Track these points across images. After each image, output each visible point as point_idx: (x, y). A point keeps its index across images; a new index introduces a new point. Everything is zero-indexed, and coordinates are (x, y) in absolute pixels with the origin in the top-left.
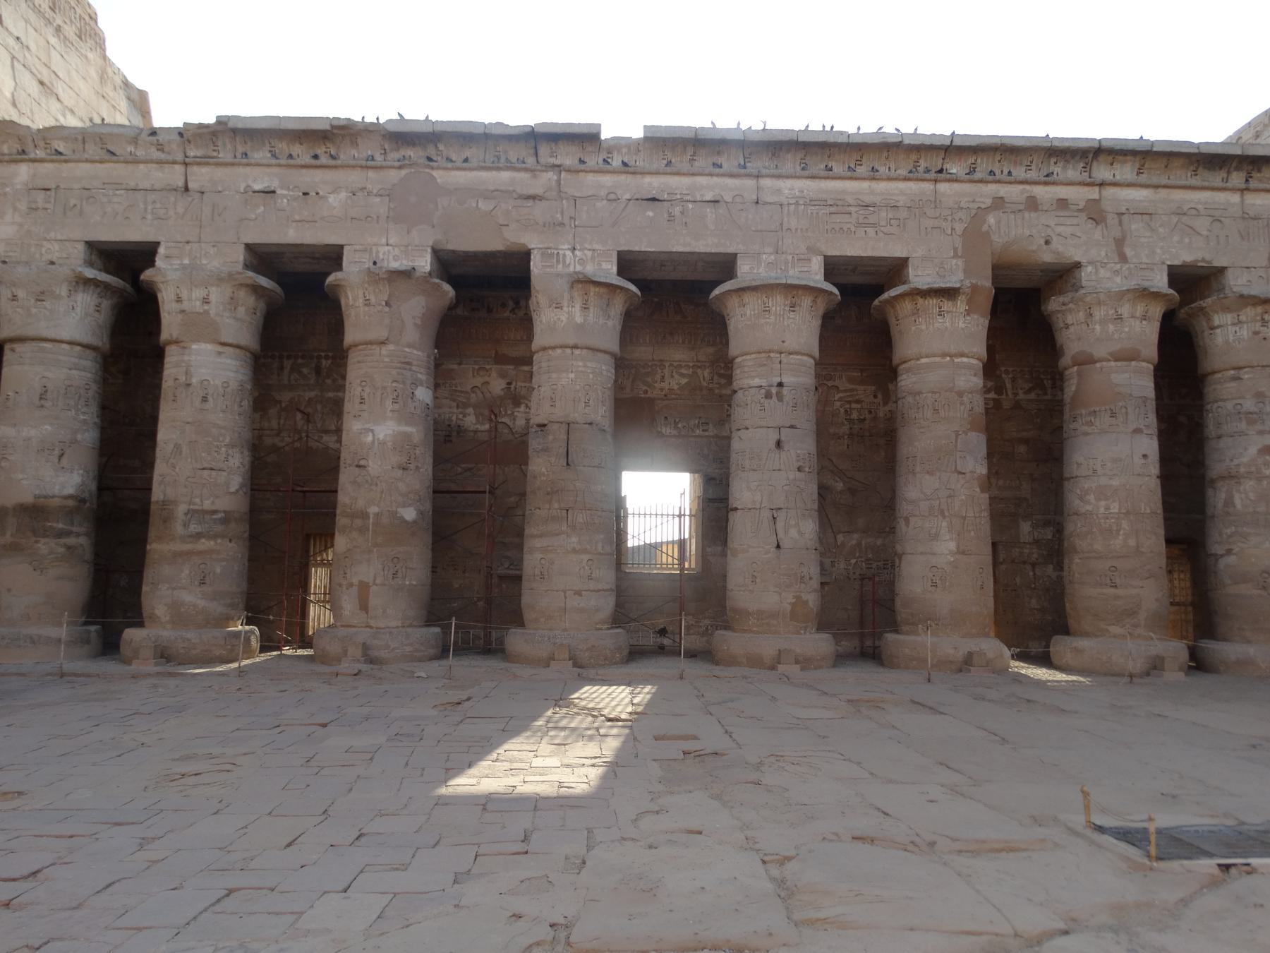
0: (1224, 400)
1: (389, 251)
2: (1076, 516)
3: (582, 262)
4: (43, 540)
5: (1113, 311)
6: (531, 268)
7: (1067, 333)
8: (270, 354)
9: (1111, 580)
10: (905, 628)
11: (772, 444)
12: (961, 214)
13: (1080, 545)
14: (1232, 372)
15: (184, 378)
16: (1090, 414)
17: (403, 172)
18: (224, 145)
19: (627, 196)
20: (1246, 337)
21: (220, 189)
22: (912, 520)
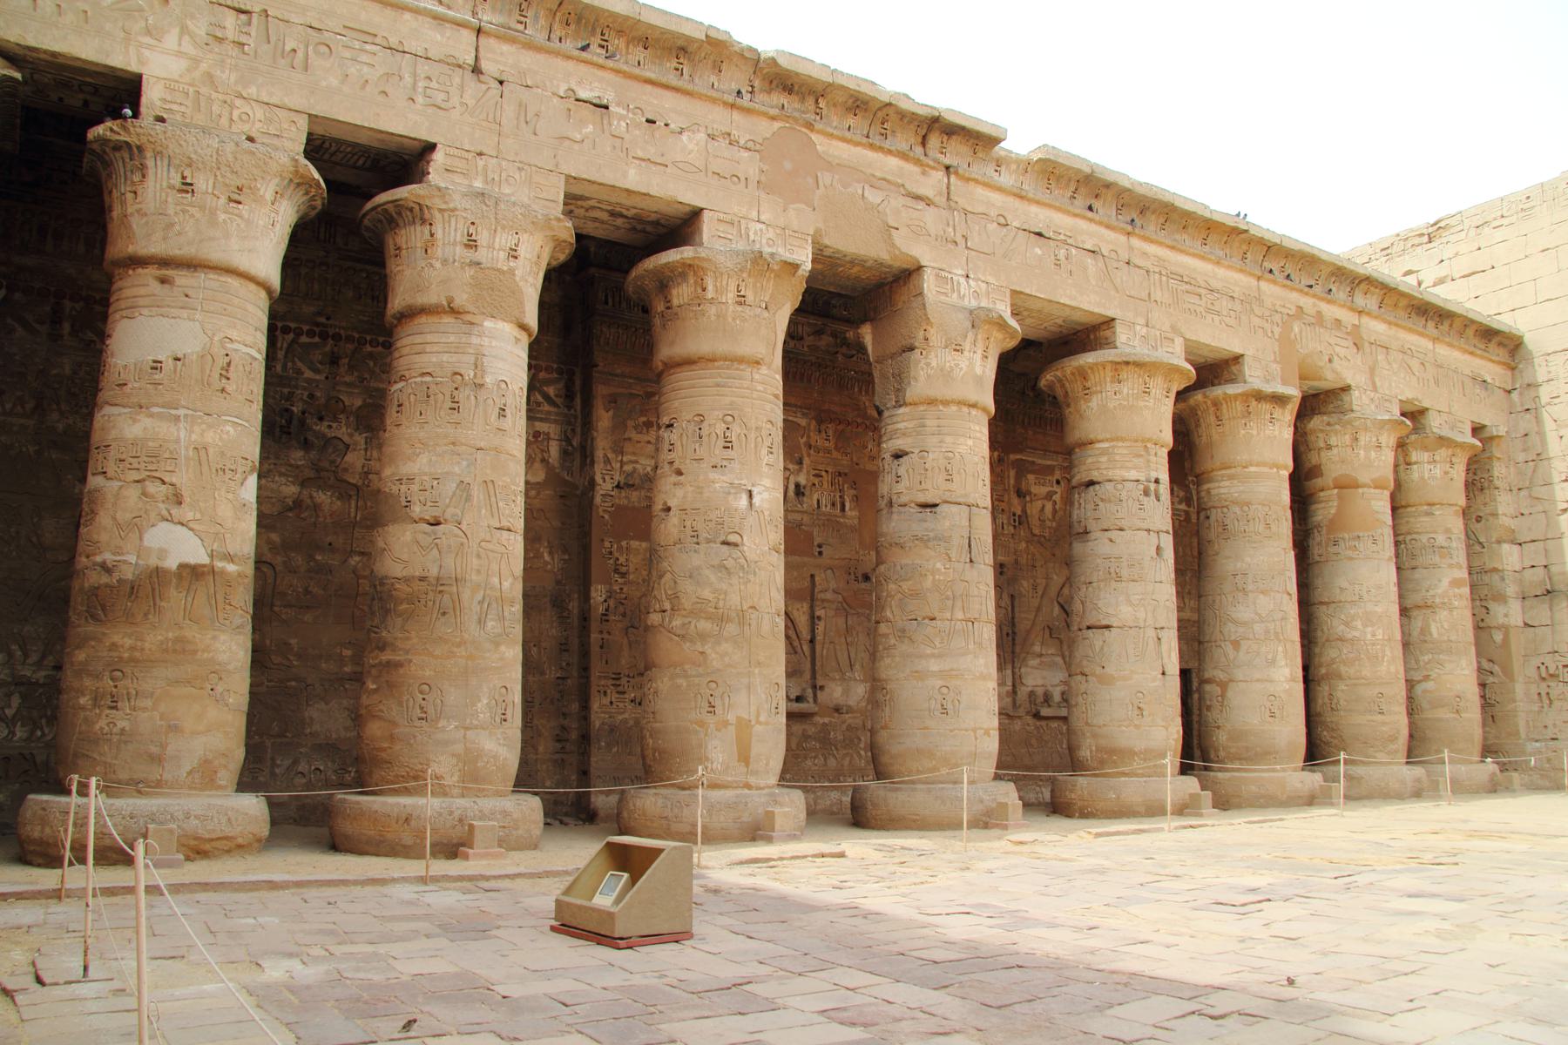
1: (761, 230)
2: (1340, 643)
3: (977, 294)
4: (223, 637)
5: (1374, 439)
6: (925, 292)
8: (381, 339)
11: (1154, 549)
12: (1277, 318)
14: (1425, 507)
15: (472, 375)
16: (1354, 539)
17: (777, 125)
18: (536, 18)
19: (1016, 224)
20: (1439, 476)
21: (529, 83)
22: (1244, 645)
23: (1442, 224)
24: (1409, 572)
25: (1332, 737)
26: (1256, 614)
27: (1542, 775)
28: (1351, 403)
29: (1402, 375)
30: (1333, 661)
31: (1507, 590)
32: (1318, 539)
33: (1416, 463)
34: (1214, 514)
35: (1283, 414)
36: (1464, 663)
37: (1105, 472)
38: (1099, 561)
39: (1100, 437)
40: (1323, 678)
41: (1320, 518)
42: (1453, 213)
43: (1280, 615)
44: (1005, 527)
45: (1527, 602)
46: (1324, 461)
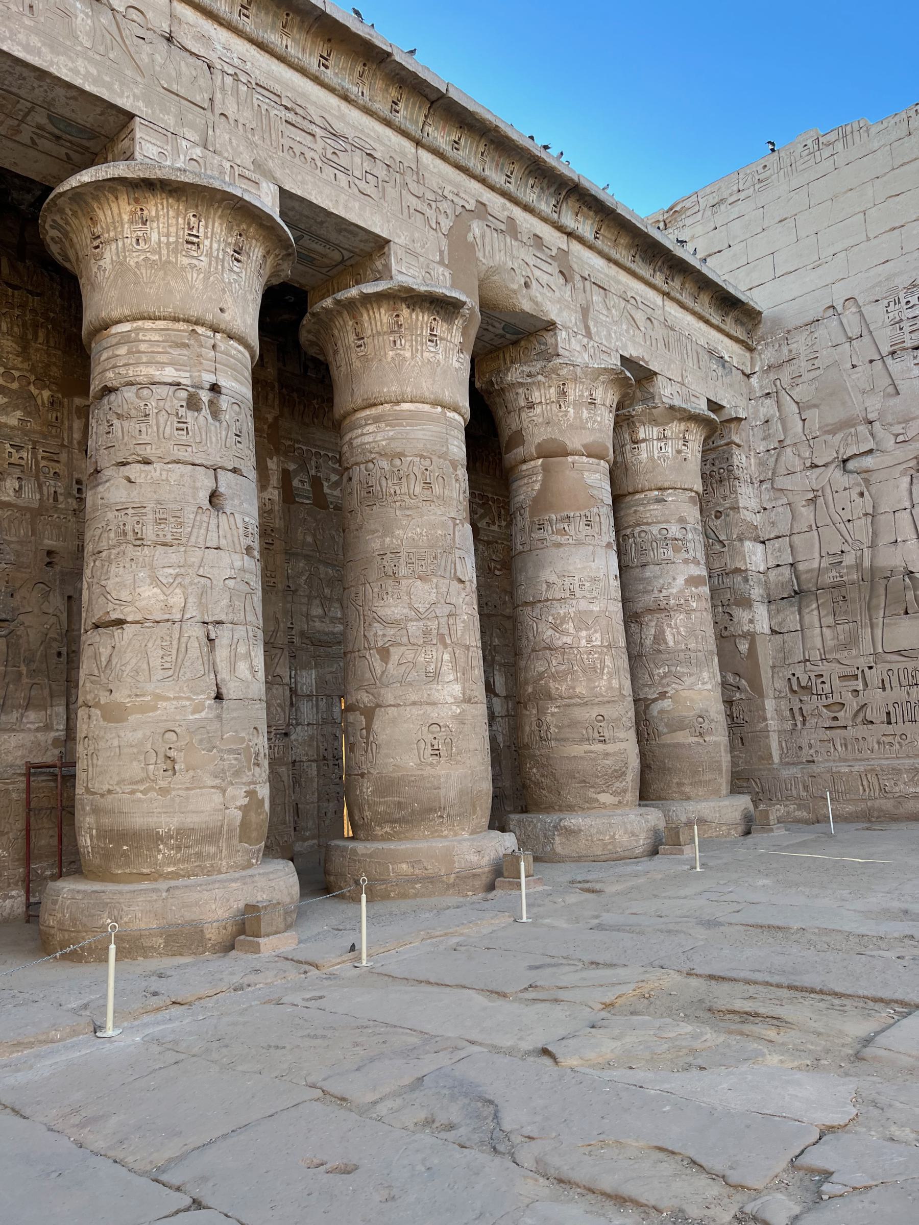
0: (648, 524)
5: (586, 394)
7: (531, 414)
9: (599, 733)
10: (378, 831)
12: (444, 206)
13: (557, 689)
14: (656, 493)
16: (562, 520)
23: (678, 208)
24: (638, 570)
25: (542, 776)
26: (411, 608)
27: (799, 805)
28: (557, 345)
29: (624, 327)
30: (541, 675)
31: (752, 592)
32: (520, 525)
33: (644, 440)
34: (358, 473)
35: (450, 331)
36: (705, 675)
37: (123, 371)
38: (110, 515)
39: (115, 314)
40: (529, 700)
41: (522, 497)
42: (688, 195)
43: (447, 609)
44: (61, 498)
45: (773, 607)
46: (525, 424)
